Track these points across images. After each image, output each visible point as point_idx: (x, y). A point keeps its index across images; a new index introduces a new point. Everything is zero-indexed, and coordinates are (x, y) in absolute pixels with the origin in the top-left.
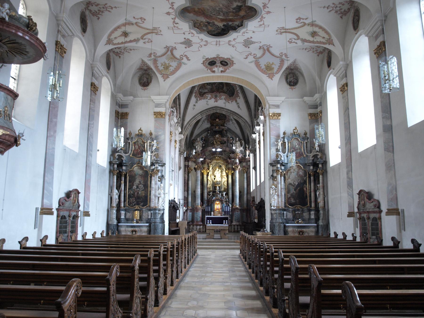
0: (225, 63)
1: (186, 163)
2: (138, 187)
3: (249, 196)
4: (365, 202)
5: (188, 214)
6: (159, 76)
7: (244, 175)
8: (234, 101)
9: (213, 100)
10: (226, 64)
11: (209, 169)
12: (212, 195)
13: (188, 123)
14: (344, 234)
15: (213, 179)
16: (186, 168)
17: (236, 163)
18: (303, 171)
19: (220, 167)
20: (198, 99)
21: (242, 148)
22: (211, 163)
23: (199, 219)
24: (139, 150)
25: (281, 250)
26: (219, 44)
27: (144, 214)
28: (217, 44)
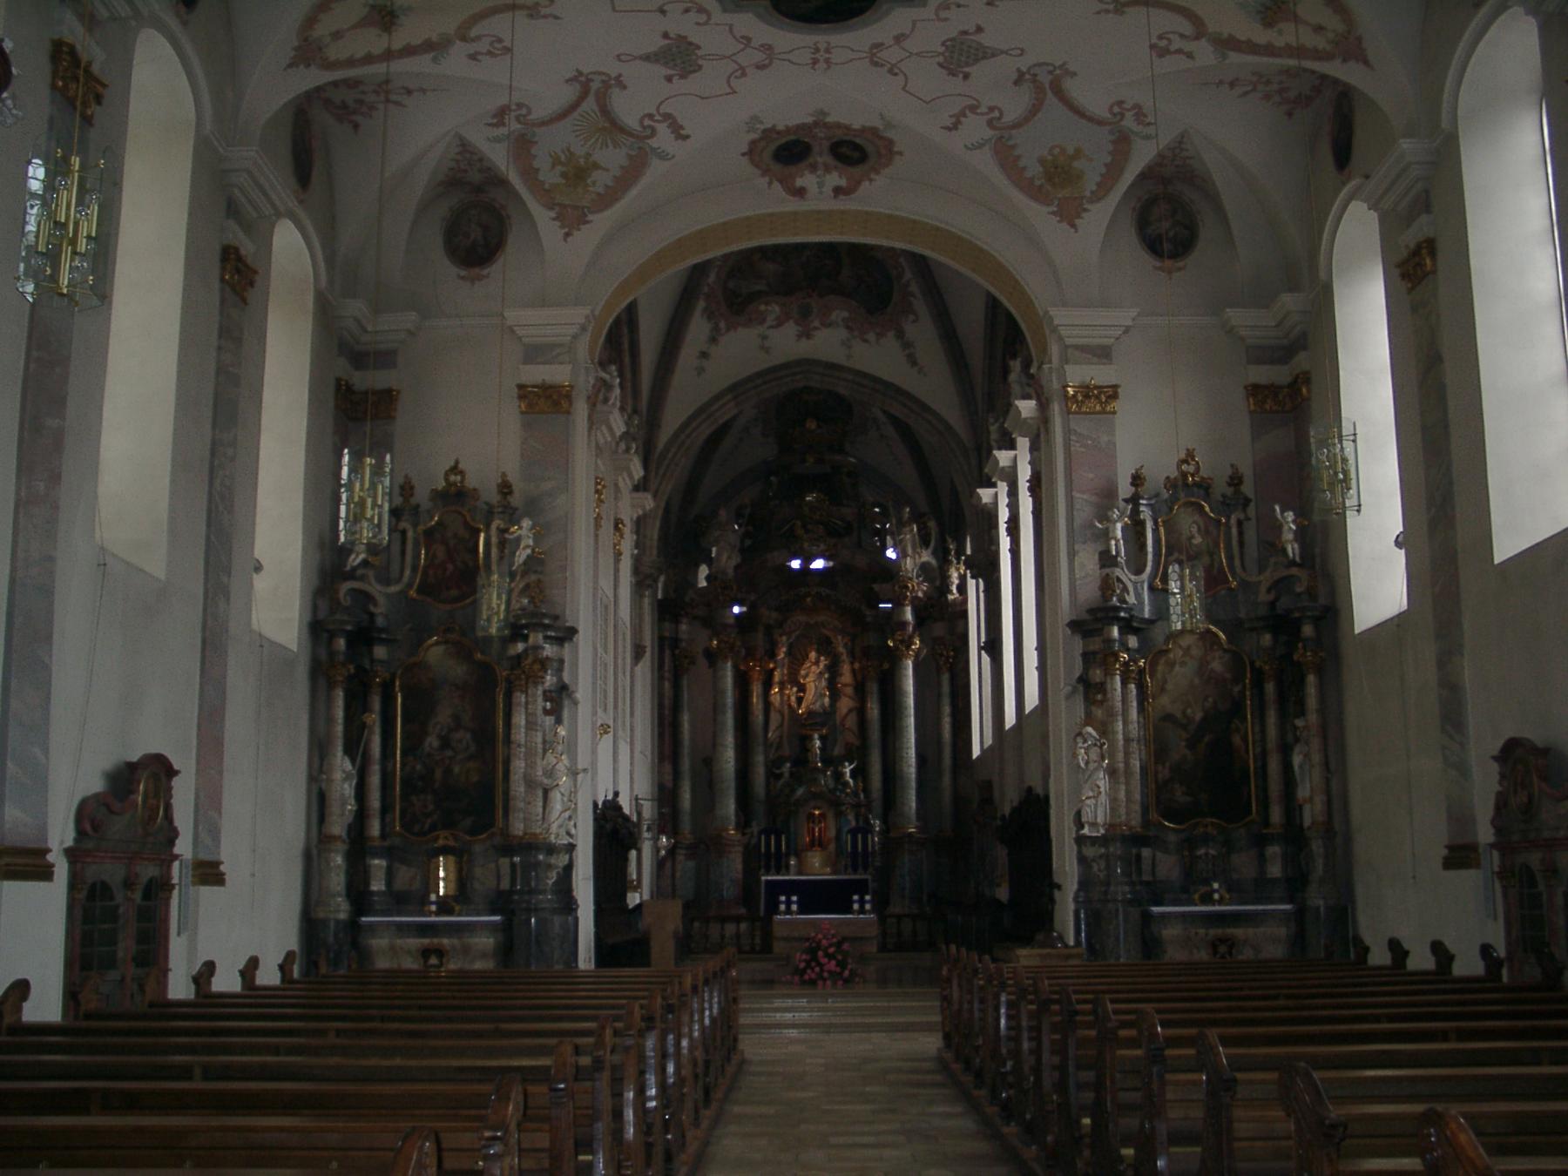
0: (854, 152)
2: (445, 743)
4: (1530, 798)
5: (679, 867)
6: (543, 217)
7: (939, 684)
8: (891, 334)
9: (791, 329)
10: (856, 155)
11: (772, 655)
12: (792, 774)
13: (676, 435)
14: (1438, 948)
15: (794, 704)
16: (667, 652)
17: (904, 624)
18: (1227, 656)
19: (825, 647)
20: (722, 325)
21: (926, 557)
23: (730, 890)
24: (450, 567)
25: (1213, 1034)
26: (827, 61)
27: (478, 871)
28: (815, 62)
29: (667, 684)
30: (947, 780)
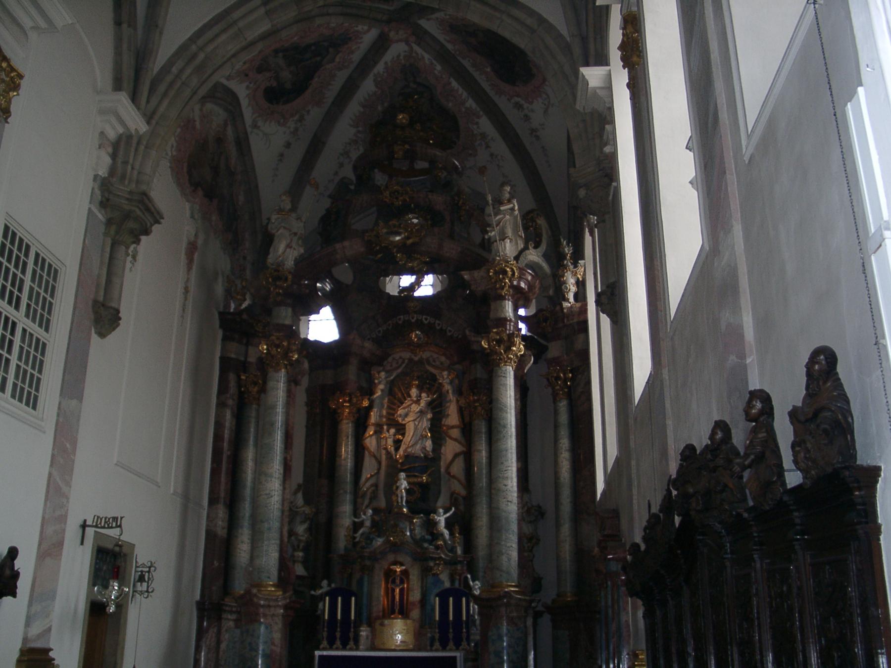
5: (226, 636)
7: (556, 412)
11: (370, 392)
12: (374, 524)
13: (184, 48)
16: (232, 377)
19: (429, 383)
21: (534, 256)
22: (380, 361)
29: (228, 415)
30: (566, 529)
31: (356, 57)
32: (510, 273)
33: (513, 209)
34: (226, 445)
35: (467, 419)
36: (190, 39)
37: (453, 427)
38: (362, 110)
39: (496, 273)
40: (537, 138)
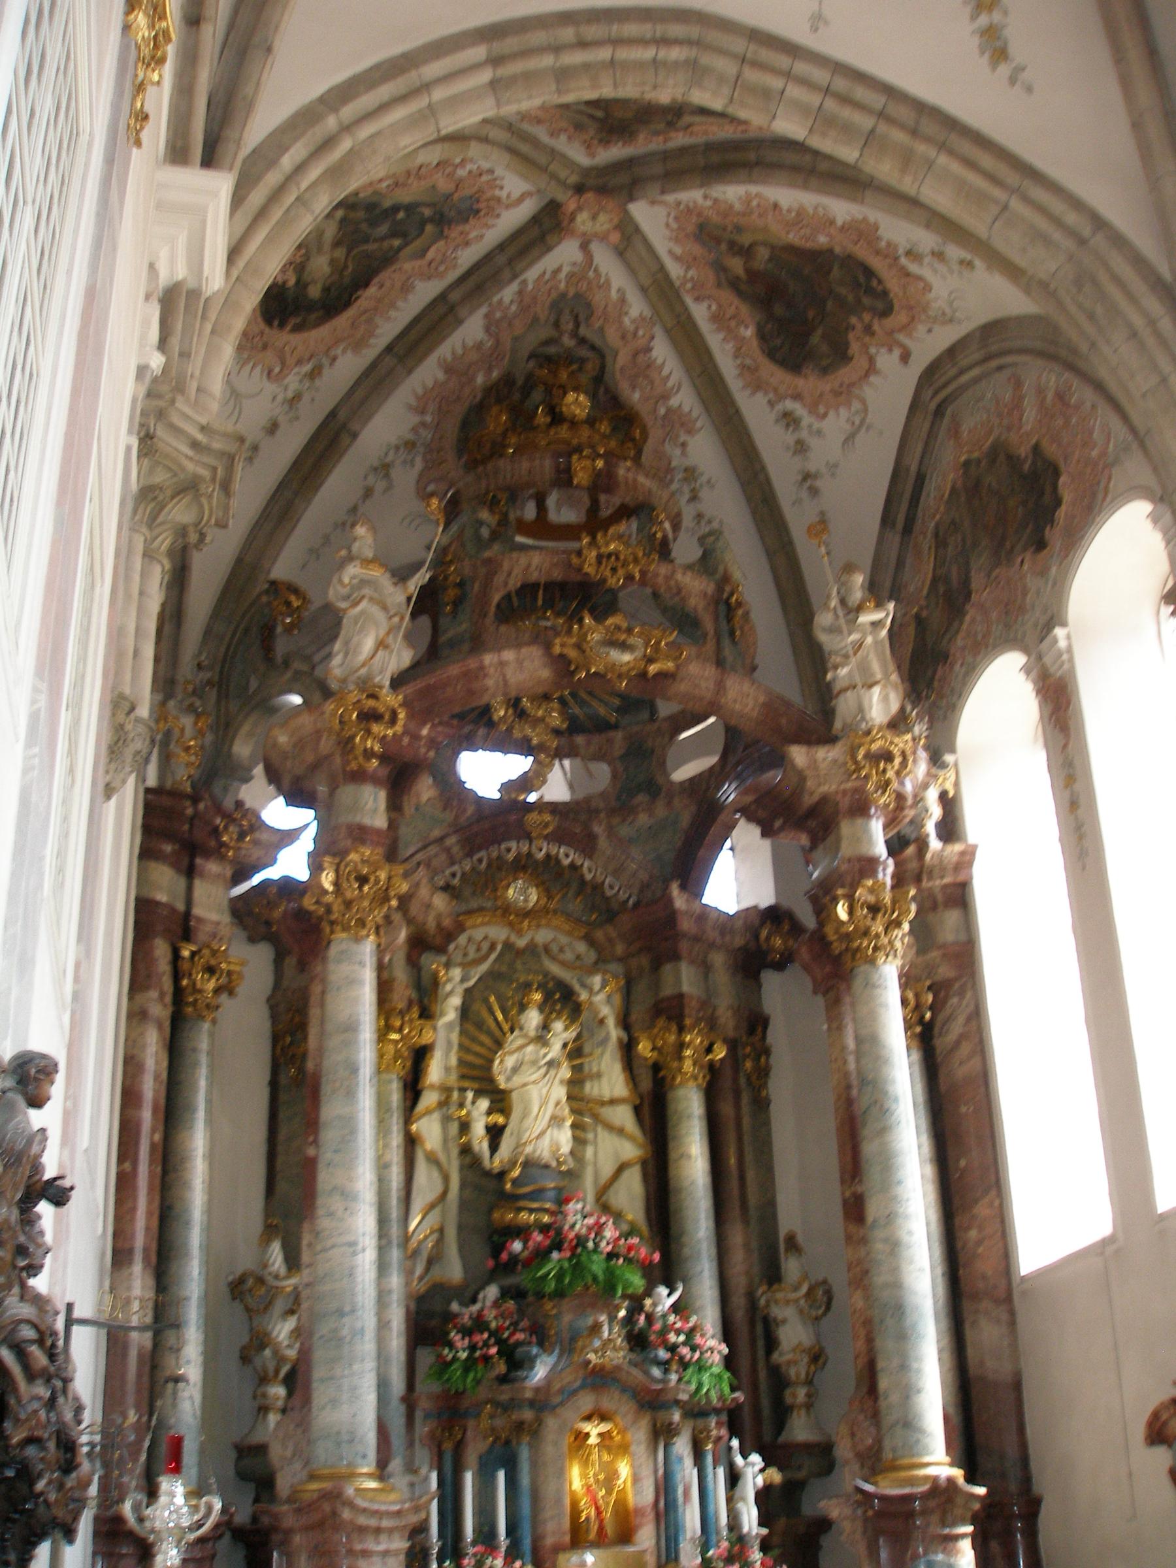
1: (166, 885)
3: (986, 1333)
13: (306, 117)
15: (480, 1143)
16: (161, 949)
19: (563, 1000)
31: (467, 257)
32: (897, 761)
33: (876, 625)
34: (146, 1116)
35: (646, 1084)
36: (322, 100)
37: (613, 1102)
38: (441, 376)
39: (867, 755)
40: (814, 492)
